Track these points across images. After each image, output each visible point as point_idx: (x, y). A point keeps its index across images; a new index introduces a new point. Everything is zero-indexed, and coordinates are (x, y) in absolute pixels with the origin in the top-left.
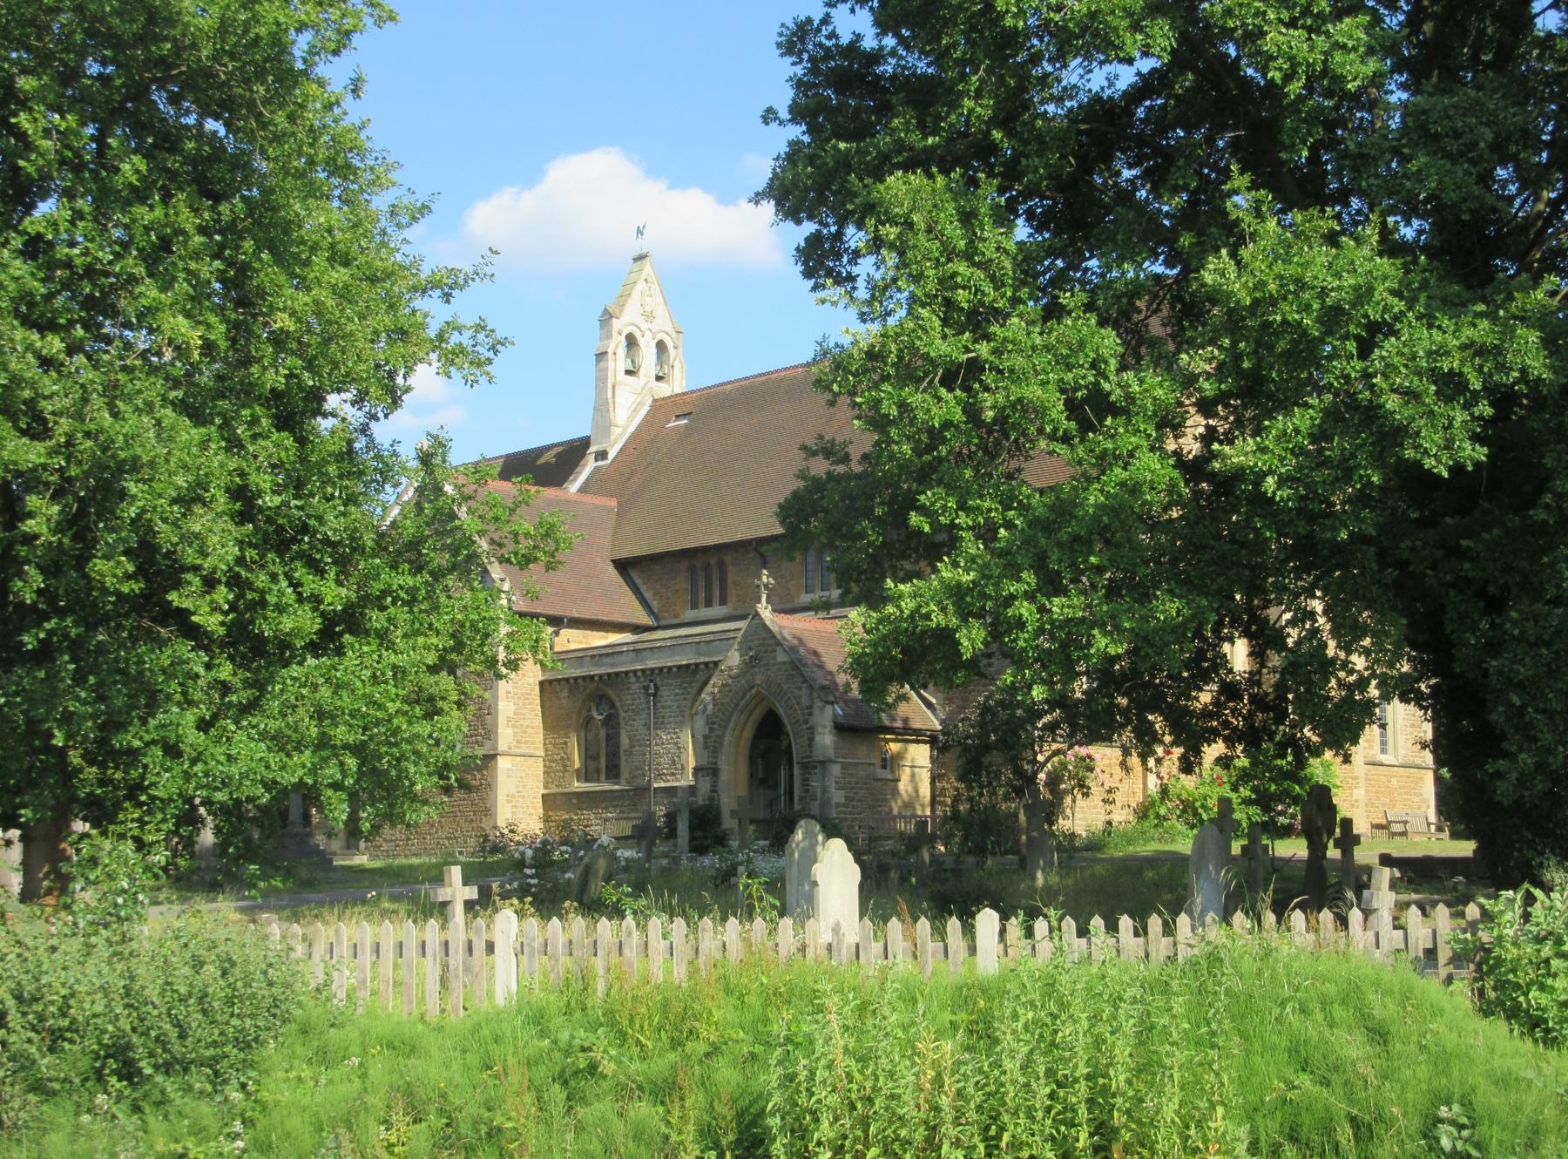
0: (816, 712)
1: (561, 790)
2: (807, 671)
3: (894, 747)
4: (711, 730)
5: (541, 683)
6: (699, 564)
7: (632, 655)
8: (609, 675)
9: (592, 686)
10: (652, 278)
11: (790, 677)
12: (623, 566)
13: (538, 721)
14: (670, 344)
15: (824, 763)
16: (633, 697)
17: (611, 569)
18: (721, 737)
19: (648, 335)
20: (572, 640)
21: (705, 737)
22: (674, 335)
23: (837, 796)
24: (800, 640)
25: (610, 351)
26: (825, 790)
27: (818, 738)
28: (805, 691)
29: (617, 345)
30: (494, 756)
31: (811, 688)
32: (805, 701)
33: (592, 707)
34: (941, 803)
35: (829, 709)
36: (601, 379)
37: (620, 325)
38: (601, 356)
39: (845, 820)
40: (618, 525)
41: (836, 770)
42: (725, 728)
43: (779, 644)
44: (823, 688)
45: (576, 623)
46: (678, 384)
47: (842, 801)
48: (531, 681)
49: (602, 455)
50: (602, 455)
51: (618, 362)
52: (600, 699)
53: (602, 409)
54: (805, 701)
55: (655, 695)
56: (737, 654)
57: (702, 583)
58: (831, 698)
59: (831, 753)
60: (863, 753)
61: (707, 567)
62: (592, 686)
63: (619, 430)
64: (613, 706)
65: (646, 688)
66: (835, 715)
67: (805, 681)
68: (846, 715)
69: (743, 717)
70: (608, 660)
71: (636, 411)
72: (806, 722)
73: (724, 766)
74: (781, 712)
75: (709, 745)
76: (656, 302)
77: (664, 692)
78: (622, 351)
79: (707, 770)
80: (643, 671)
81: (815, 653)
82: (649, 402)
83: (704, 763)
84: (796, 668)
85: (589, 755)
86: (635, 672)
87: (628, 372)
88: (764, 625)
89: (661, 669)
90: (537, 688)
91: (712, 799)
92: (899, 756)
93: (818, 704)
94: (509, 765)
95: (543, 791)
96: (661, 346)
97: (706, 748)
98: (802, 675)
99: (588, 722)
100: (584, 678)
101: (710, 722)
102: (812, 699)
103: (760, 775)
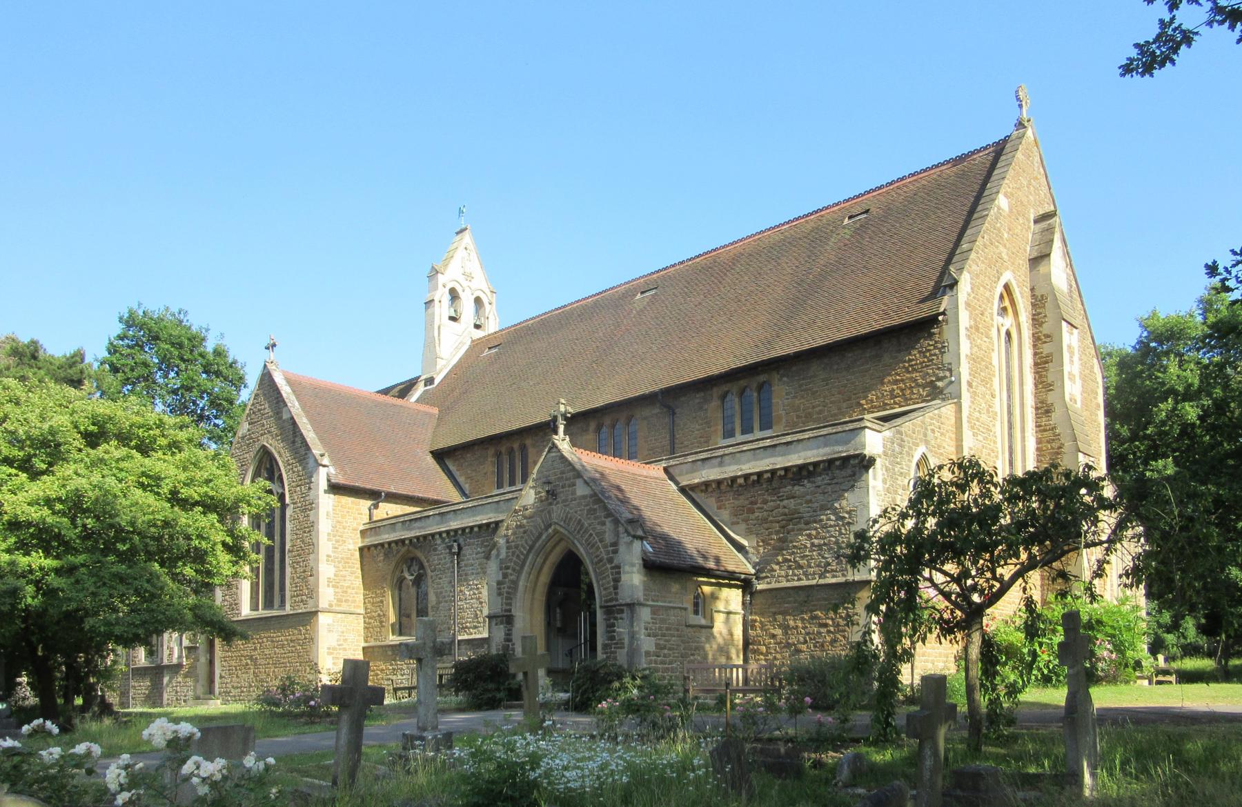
0: (622, 548)
2: (612, 505)
3: (707, 589)
4: (505, 576)
6: (503, 449)
7: (438, 518)
8: (418, 538)
9: (404, 550)
10: (471, 247)
11: (592, 512)
12: (440, 456)
14: (485, 301)
15: (631, 606)
16: (439, 558)
18: (515, 583)
20: (388, 510)
21: (499, 583)
22: (489, 294)
23: (647, 644)
24: (602, 474)
26: (633, 636)
27: (624, 577)
28: (609, 525)
29: (442, 295)
31: (616, 522)
32: (609, 538)
33: (402, 564)
34: (755, 652)
35: (637, 545)
36: (430, 322)
37: (445, 280)
38: (429, 303)
39: (656, 670)
40: (438, 425)
41: (645, 614)
42: (519, 573)
43: (578, 475)
44: (631, 522)
45: (393, 498)
46: (492, 326)
47: (653, 649)
49: (430, 381)
50: (430, 381)
51: (443, 309)
52: (411, 561)
53: (430, 346)
54: (609, 538)
55: (458, 554)
56: (532, 492)
57: (506, 466)
58: (640, 533)
59: (640, 595)
60: (677, 595)
61: (511, 452)
62: (404, 550)
65: (450, 548)
66: (644, 552)
68: (655, 553)
70: (417, 524)
72: (610, 560)
74: (582, 551)
75: (505, 590)
76: (475, 267)
77: (467, 551)
78: (447, 297)
79: (503, 618)
80: (448, 532)
81: (619, 488)
82: (469, 343)
83: (498, 610)
84: (599, 501)
85: (402, 613)
86: (440, 534)
87: (453, 319)
88: (563, 458)
89: (463, 529)
92: (714, 597)
93: (625, 539)
96: (478, 301)
97: (500, 594)
98: (606, 508)
99: (399, 584)
100: (396, 542)
101: (503, 567)
102: (617, 535)
103: (559, 624)
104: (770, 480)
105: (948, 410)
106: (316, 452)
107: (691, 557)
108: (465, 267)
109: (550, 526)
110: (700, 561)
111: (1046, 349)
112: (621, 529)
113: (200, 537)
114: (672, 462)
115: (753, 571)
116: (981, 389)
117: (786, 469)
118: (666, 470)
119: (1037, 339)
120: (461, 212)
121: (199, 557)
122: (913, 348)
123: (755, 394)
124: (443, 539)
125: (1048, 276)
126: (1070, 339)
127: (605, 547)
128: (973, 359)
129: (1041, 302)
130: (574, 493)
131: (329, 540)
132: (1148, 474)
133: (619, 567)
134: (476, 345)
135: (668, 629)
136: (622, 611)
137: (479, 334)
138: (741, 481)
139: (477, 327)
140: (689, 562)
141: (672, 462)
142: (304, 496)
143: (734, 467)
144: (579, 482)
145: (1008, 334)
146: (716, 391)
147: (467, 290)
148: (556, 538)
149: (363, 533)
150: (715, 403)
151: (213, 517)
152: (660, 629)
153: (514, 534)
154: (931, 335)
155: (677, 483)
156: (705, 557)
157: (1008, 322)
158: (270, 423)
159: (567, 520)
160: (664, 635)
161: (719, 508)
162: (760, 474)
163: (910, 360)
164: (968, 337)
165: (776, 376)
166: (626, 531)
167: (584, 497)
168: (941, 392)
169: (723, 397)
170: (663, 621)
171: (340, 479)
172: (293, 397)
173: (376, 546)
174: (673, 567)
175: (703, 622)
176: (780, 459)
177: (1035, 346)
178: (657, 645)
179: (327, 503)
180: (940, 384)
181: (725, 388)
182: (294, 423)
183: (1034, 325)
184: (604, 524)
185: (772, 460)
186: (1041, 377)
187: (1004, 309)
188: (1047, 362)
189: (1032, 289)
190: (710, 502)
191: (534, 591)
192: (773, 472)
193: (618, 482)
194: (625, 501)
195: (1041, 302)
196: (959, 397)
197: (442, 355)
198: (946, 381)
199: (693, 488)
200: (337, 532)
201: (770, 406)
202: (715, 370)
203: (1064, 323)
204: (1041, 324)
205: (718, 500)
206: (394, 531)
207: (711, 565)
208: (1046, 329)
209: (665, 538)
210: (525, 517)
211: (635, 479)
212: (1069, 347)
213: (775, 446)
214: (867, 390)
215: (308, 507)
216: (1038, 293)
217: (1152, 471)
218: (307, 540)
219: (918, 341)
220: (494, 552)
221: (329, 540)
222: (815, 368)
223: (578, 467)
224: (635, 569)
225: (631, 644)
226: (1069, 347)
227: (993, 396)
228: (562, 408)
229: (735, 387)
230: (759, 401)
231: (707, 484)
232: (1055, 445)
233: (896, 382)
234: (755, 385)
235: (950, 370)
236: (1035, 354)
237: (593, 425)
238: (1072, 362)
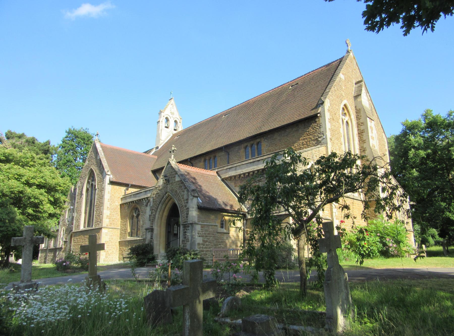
0: (190, 201)
1: (124, 240)
2: (187, 184)
3: (227, 218)
4: (152, 213)
5: (121, 205)
7: (144, 193)
8: (138, 200)
10: (174, 104)
13: (119, 217)
17: (151, 173)
18: (155, 215)
20: (131, 190)
23: (199, 240)
24: (188, 173)
25: (161, 121)
26: (192, 237)
27: (190, 213)
29: (163, 120)
30: (101, 228)
31: (188, 191)
32: (185, 197)
35: (195, 200)
38: (158, 122)
41: (198, 228)
42: (156, 212)
43: (176, 172)
44: (193, 190)
45: (133, 186)
47: (201, 242)
48: (117, 204)
49: (157, 148)
50: (157, 148)
51: (163, 124)
53: (158, 136)
54: (185, 197)
58: (196, 195)
59: (196, 220)
63: (162, 141)
64: (139, 211)
66: (198, 202)
67: (186, 188)
69: (163, 206)
70: (138, 195)
71: (168, 137)
72: (186, 206)
73: (155, 228)
76: (175, 110)
78: (164, 120)
81: (194, 179)
82: (172, 135)
84: (183, 183)
86: (145, 198)
87: (166, 127)
88: (172, 167)
90: (119, 207)
91: (151, 241)
93: (191, 197)
94: (107, 231)
95: (119, 240)
96: (176, 122)
98: (185, 186)
99: (132, 218)
100: (131, 202)
101: (152, 210)
102: (188, 196)
104: (253, 175)
106: (106, 170)
107: (220, 205)
108: (171, 110)
109: (166, 193)
110: (223, 206)
111: (362, 128)
112: (189, 194)
113: (35, 198)
114: (219, 170)
115: (247, 211)
116: (336, 141)
117: (258, 171)
118: (217, 172)
119: (358, 125)
120: (171, 93)
121: (36, 206)
122: (310, 127)
123: (256, 146)
124: (146, 201)
125: (361, 102)
126: (370, 124)
127: (184, 201)
128: (332, 130)
129: (359, 111)
130: (175, 180)
131: (108, 201)
133: (188, 209)
134: (174, 136)
135: (208, 234)
136: (189, 226)
137: (176, 132)
138: (242, 176)
139: (175, 130)
140: (218, 207)
141: (219, 170)
142: (101, 185)
143: (240, 171)
144: (176, 176)
145: (347, 122)
146: (243, 146)
147: (172, 118)
148: (169, 198)
149: (122, 199)
150: (242, 150)
151: (43, 191)
152: (205, 234)
153: (155, 196)
154: (316, 122)
155: (221, 177)
156: (226, 205)
157: (347, 118)
158: (94, 161)
159: (172, 190)
160: (206, 236)
161: (235, 186)
162: (249, 173)
163: (309, 131)
164: (330, 122)
165: (262, 139)
166: (191, 194)
167: (178, 181)
168: (320, 142)
169: (246, 148)
170: (206, 230)
171: (114, 180)
172: (102, 152)
173: (125, 203)
174: (211, 209)
175: (225, 231)
176: (256, 167)
177: (358, 127)
178: (203, 240)
179: (108, 188)
180: (320, 139)
181: (246, 144)
182: (101, 161)
183: (357, 120)
184: (184, 192)
185: (253, 167)
186: (361, 138)
187: (345, 114)
188: (362, 133)
189: (356, 107)
190: (232, 184)
191: (161, 219)
192: (253, 172)
193: (195, 176)
194: (195, 183)
195: (359, 111)
196: (327, 144)
197: (162, 139)
198: (322, 138)
199: (226, 179)
200: (112, 199)
201: (261, 150)
202: (242, 138)
204: (359, 119)
205: (235, 183)
206: (131, 198)
207: (228, 208)
208: (361, 121)
209: (210, 198)
210: (159, 190)
211: (203, 175)
212: (371, 127)
213: (254, 162)
214: (294, 143)
215: (102, 190)
216: (358, 108)
218: (101, 202)
219: (311, 124)
220: (149, 204)
221: (108, 201)
222: (276, 136)
223: (177, 170)
224: (194, 209)
225: (191, 240)
226: (371, 127)
227: (341, 144)
228: (173, 148)
229: (249, 144)
230: (258, 148)
231: (231, 177)
233: (304, 139)
234: (255, 143)
235: (323, 134)
236: (358, 130)
237: (203, 160)
238: (372, 132)
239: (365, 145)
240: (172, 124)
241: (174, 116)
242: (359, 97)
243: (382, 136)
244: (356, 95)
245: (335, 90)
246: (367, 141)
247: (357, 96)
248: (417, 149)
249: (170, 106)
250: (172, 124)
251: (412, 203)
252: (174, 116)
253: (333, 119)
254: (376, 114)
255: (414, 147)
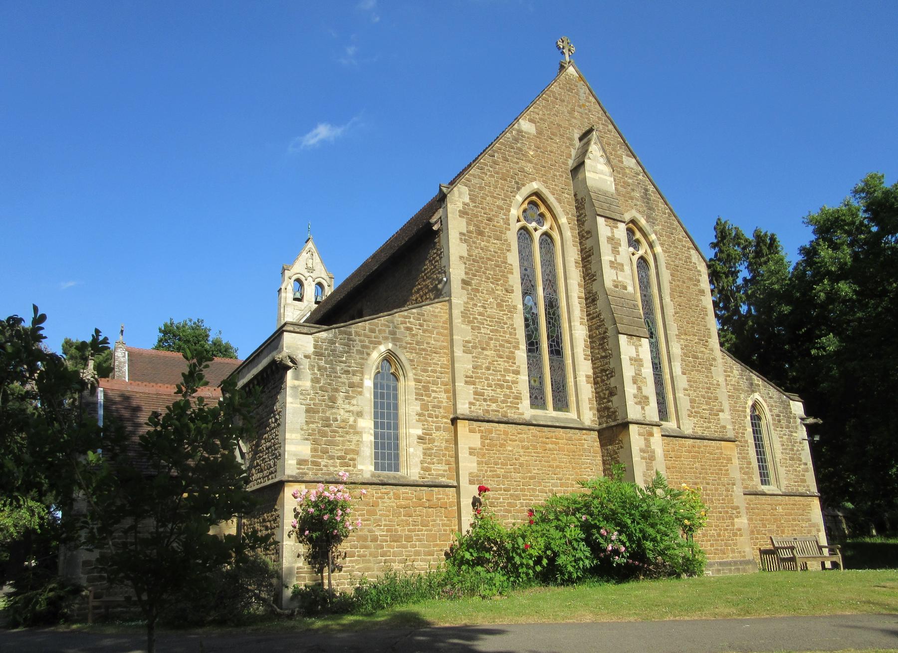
10: (314, 249)
19: (310, 279)
22: (328, 279)
51: (288, 295)
87: (295, 299)
96: (320, 285)
105: (435, 310)
111: (588, 244)
132: (813, 352)
147: (310, 279)
163: (425, 269)
177: (580, 243)
180: (440, 286)
183: (579, 226)
186: (586, 270)
187: (542, 215)
188: (590, 256)
189: (575, 195)
203: (601, 221)
204: (583, 224)
208: (586, 227)
216: (579, 197)
217: (818, 349)
232: (601, 330)
233: (418, 292)
235: (445, 272)
239: (595, 287)
240: (310, 292)
241: (314, 275)
242: (581, 170)
243: (689, 257)
244: (575, 165)
245: (495, 163)
246: (598, 274)
247: (579, 167)
248: (835, 278)
249: (304, 256)
250: (310, 292)
251: (811, 420)
252: (314, 275)
253: (481, 233)
254: (662, 205)
255: (829, 273)
